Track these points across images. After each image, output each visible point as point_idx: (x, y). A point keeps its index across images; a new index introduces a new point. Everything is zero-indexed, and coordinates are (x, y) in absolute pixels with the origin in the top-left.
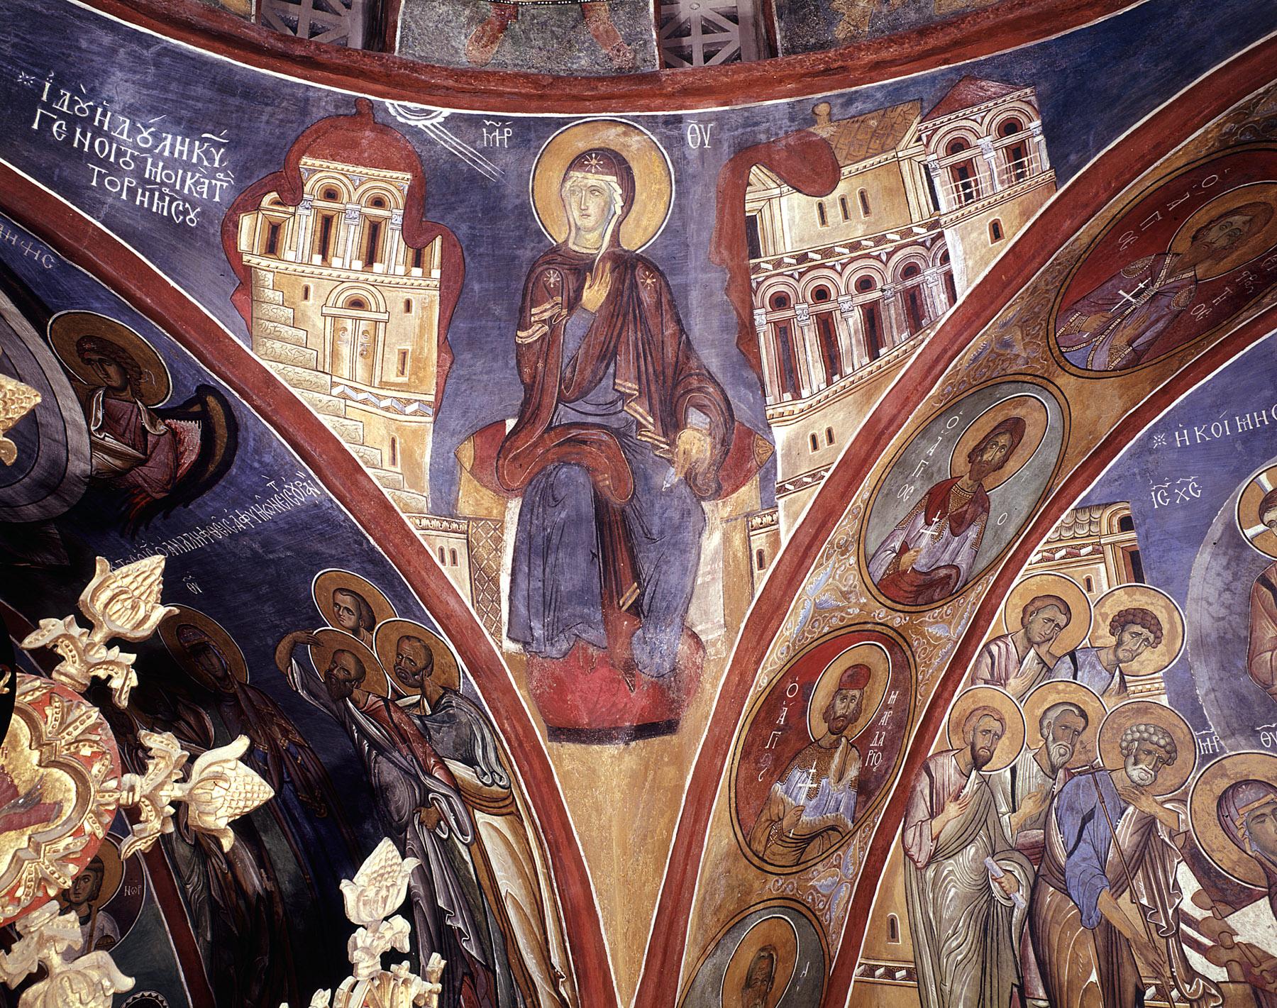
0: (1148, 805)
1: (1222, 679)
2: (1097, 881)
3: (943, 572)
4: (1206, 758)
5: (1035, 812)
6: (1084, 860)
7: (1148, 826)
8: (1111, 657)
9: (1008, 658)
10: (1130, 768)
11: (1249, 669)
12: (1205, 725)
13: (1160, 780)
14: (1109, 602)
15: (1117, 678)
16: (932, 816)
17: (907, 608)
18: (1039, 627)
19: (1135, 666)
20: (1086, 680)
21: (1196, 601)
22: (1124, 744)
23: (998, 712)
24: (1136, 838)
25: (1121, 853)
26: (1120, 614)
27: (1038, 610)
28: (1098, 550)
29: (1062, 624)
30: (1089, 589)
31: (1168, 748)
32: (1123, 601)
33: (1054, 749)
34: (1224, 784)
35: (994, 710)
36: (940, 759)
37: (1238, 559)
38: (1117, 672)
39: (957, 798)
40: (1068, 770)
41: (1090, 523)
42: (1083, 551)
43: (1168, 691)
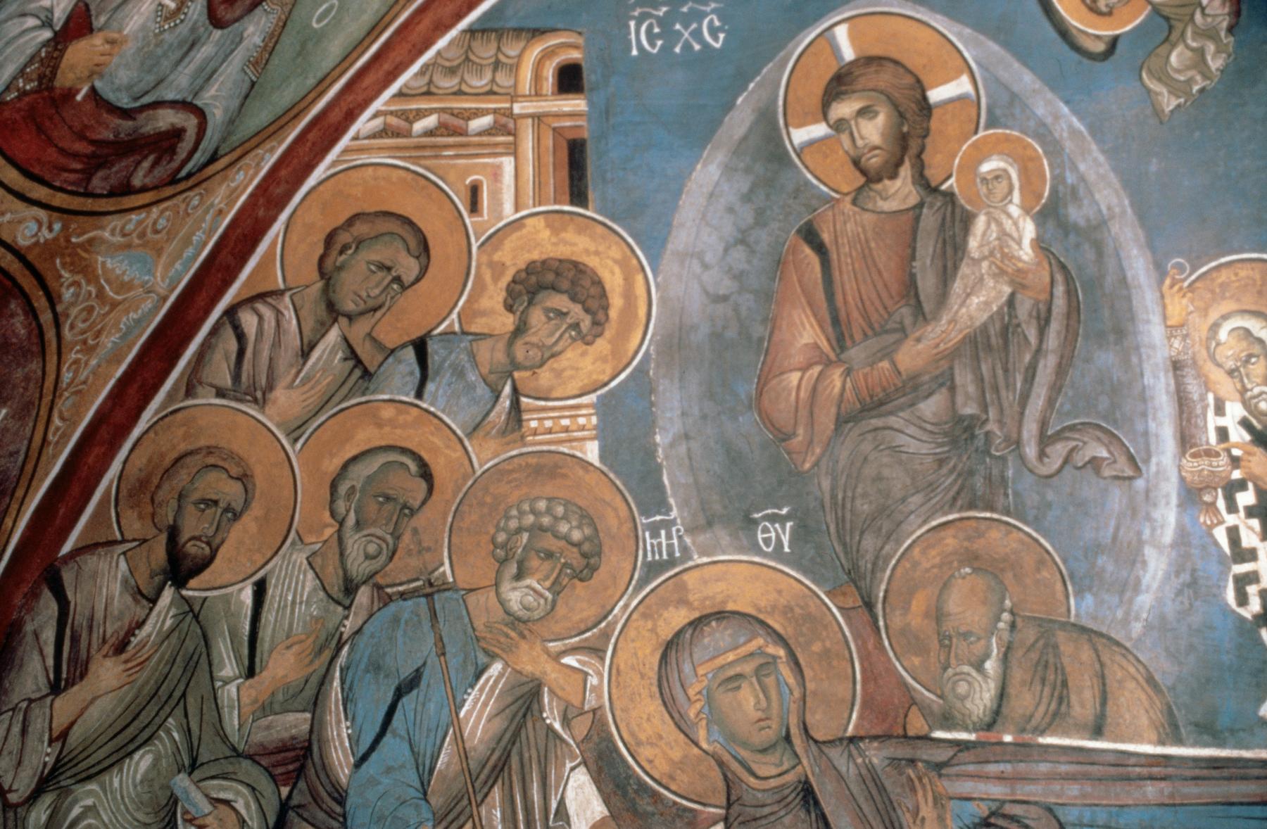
0: (531, 660)
1: (704, 417)
2: (409, 813)
3: (166, 119)
4: (654, 569)
5: (296, 676)
6: (389, 770)
7: (525, 700)
8: (500, 356)
9: (277, 344)
10: (506, 586)
11: (757, 402)
12: (663, 507)
13: (561, 610)
14: (510, 243)
15: (505, 402)
16: (56, 688)
17: (60, 199)
18: (356, 283)
19: (545, 377)
20: (441, 401)
21: (683, 257)
22: (501, 537)
23: (240, 461)
24: (499, 724)
25: (465, 755)
26: (530, 269)
27: (360, 243)
28: (505, 126)
29: (408, 278)
30: (474, 207)
31: (586, 547)
32: (543, 242)
33: (356, 545)
34: (678, 618)
35: (231, 456)
36: (91, 562)
37: (766, 184)
38: (507, 389)
39: (121, 647)
40: (379, 588)
41: (497, 65)
42: (477, 124)
43: (602, 433)
